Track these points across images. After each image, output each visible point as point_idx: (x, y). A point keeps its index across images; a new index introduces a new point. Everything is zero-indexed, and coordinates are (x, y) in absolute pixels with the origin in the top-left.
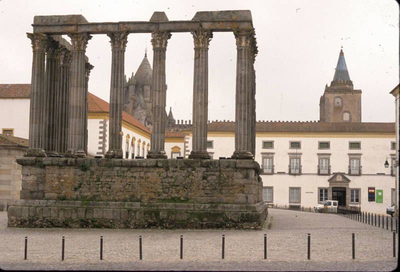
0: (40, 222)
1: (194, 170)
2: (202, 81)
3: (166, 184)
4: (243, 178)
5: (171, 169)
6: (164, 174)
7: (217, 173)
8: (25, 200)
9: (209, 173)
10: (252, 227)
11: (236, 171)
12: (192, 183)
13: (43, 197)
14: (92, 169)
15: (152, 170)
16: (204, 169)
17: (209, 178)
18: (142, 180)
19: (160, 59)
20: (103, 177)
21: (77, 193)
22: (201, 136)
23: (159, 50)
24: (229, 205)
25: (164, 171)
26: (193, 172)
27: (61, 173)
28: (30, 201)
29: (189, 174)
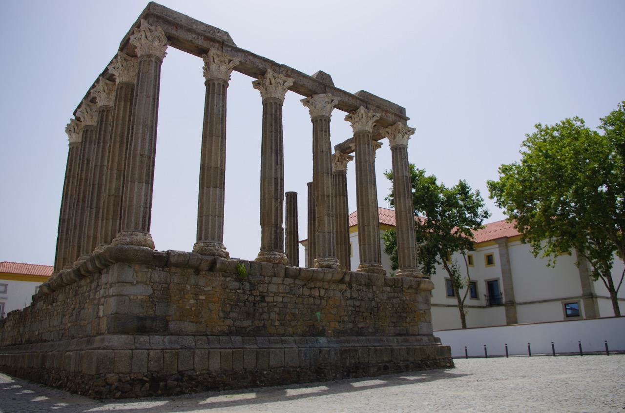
0: (176, 383)
3: (351, 308)
8: (131, 337)
9: (392, 295)
10: (448, 365)
11: (417, 294)
12: (378, 308)
13: (165, 330)
15: (333, 286)
16: (388, 289)
20: (271, 294)
21: (229, 322)
24: (418, 337)
25: (348, 288)
27: (200, 284)
28: (144, 338)
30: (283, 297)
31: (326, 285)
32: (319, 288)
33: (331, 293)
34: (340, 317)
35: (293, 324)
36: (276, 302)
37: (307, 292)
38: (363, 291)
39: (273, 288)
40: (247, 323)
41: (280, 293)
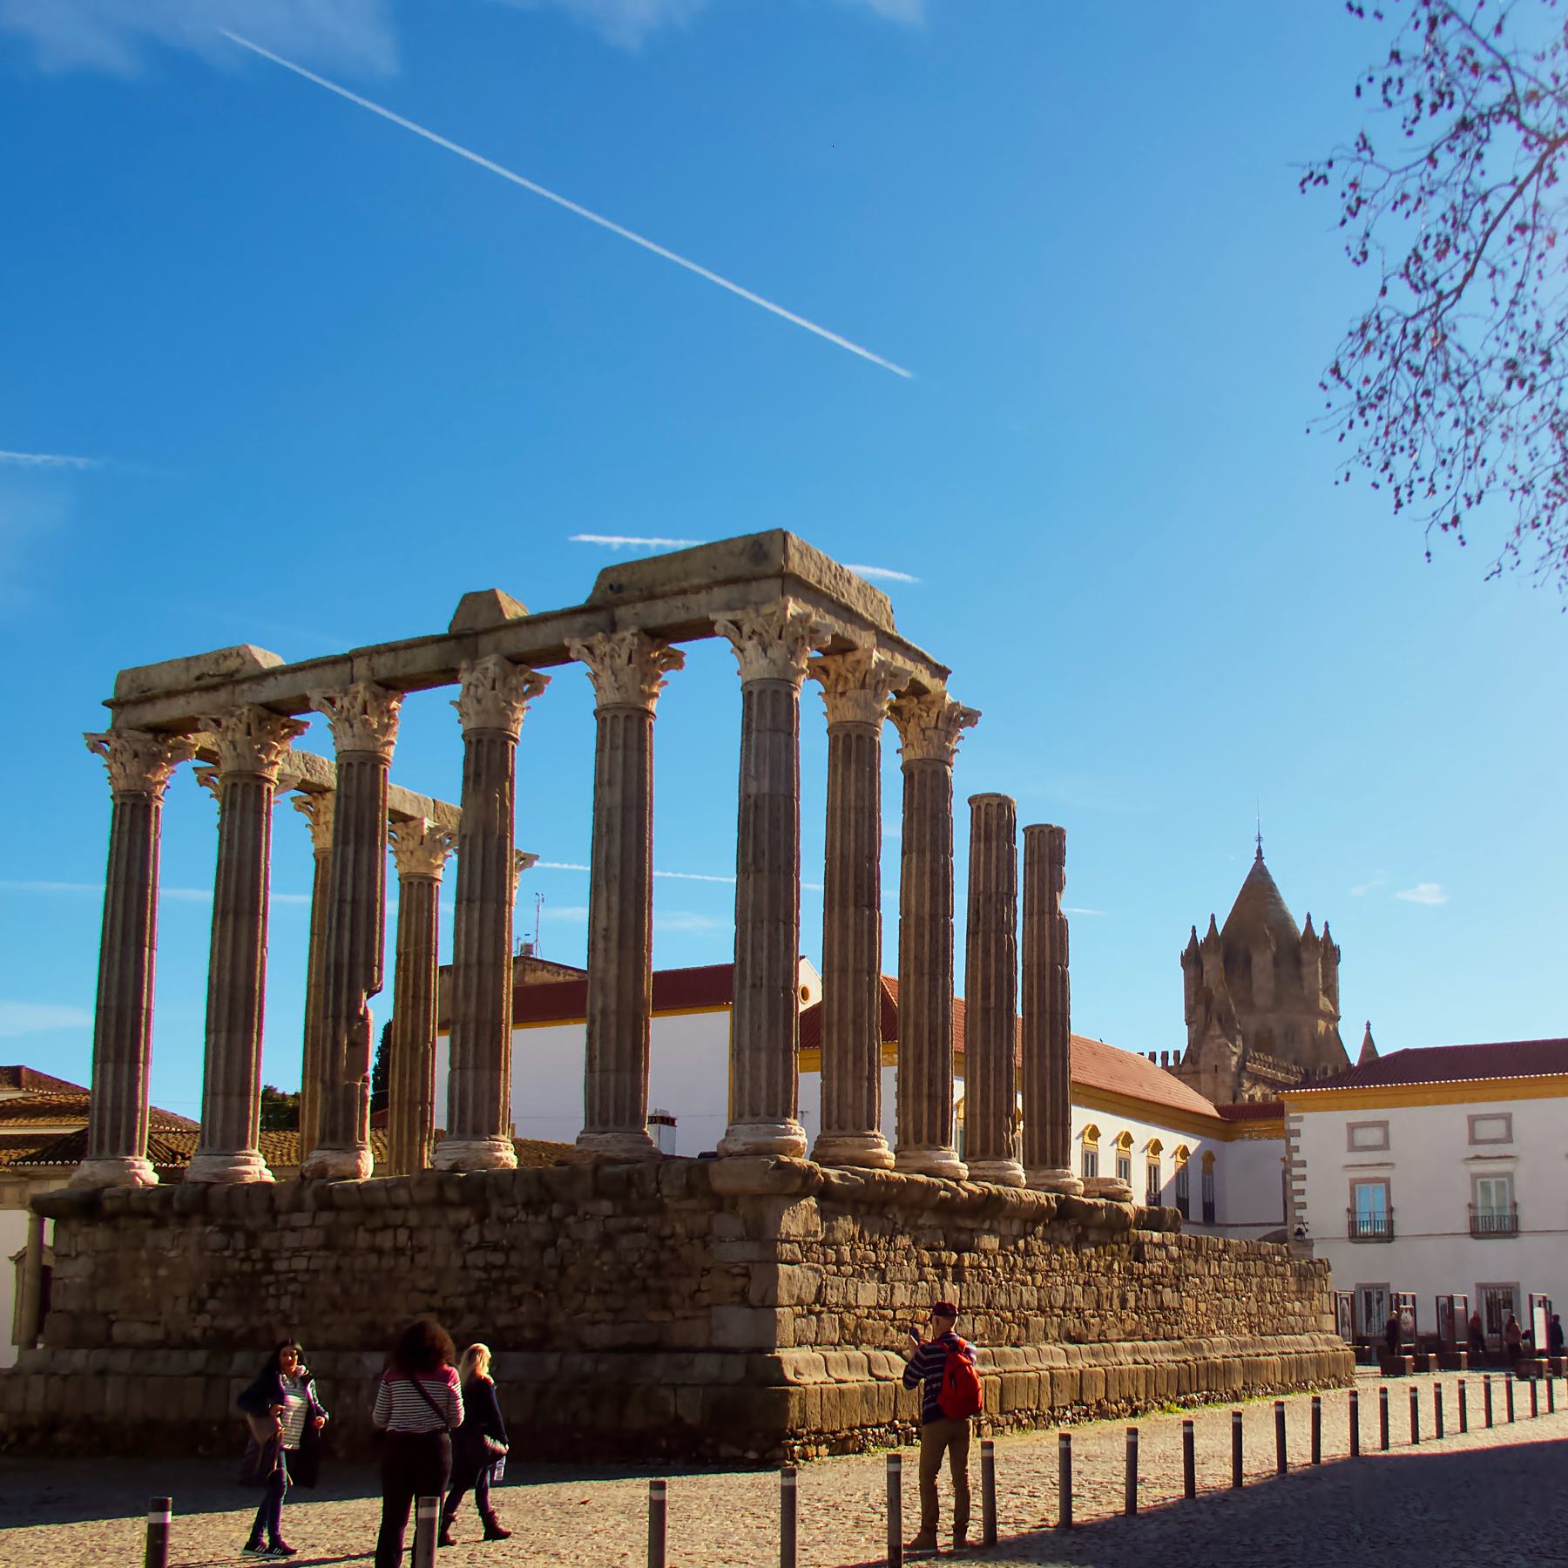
1: (575, 1214)
2: (610, 842)
3: (478, 1274)
4: (740, 1239)
5: (495, 1208)
6: (472, 1236)
7: (652, 1221)
11: (719, 1209)
12: (562, 1269)
14: (250, 1223)
16: (606, 1206)
17: (625, 1242)
18: (404, 1262)
19: (477, 775)
21: (204, 1320)
22: (604, 1070)
23: (474, 739)
26: (571, 1220)
29: (556, 1224)
30: (310, 1258)
31: (413, 1218)
32: (396, 1227)
33: (425, 1238)
34: (445, 1298)
35: (327, 1319)
36: (295, 1271)
37: (363, 1239)
38: (520, 1222)
39: (291, 1240)
40: (232, 1322)
41: (306, 1249)
